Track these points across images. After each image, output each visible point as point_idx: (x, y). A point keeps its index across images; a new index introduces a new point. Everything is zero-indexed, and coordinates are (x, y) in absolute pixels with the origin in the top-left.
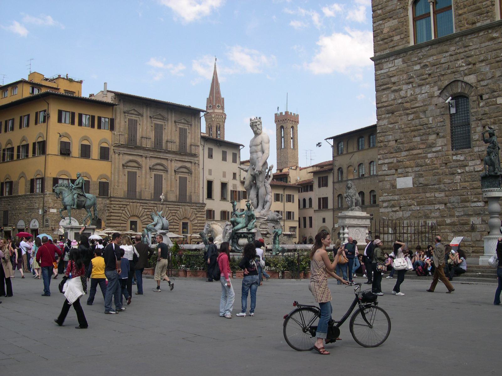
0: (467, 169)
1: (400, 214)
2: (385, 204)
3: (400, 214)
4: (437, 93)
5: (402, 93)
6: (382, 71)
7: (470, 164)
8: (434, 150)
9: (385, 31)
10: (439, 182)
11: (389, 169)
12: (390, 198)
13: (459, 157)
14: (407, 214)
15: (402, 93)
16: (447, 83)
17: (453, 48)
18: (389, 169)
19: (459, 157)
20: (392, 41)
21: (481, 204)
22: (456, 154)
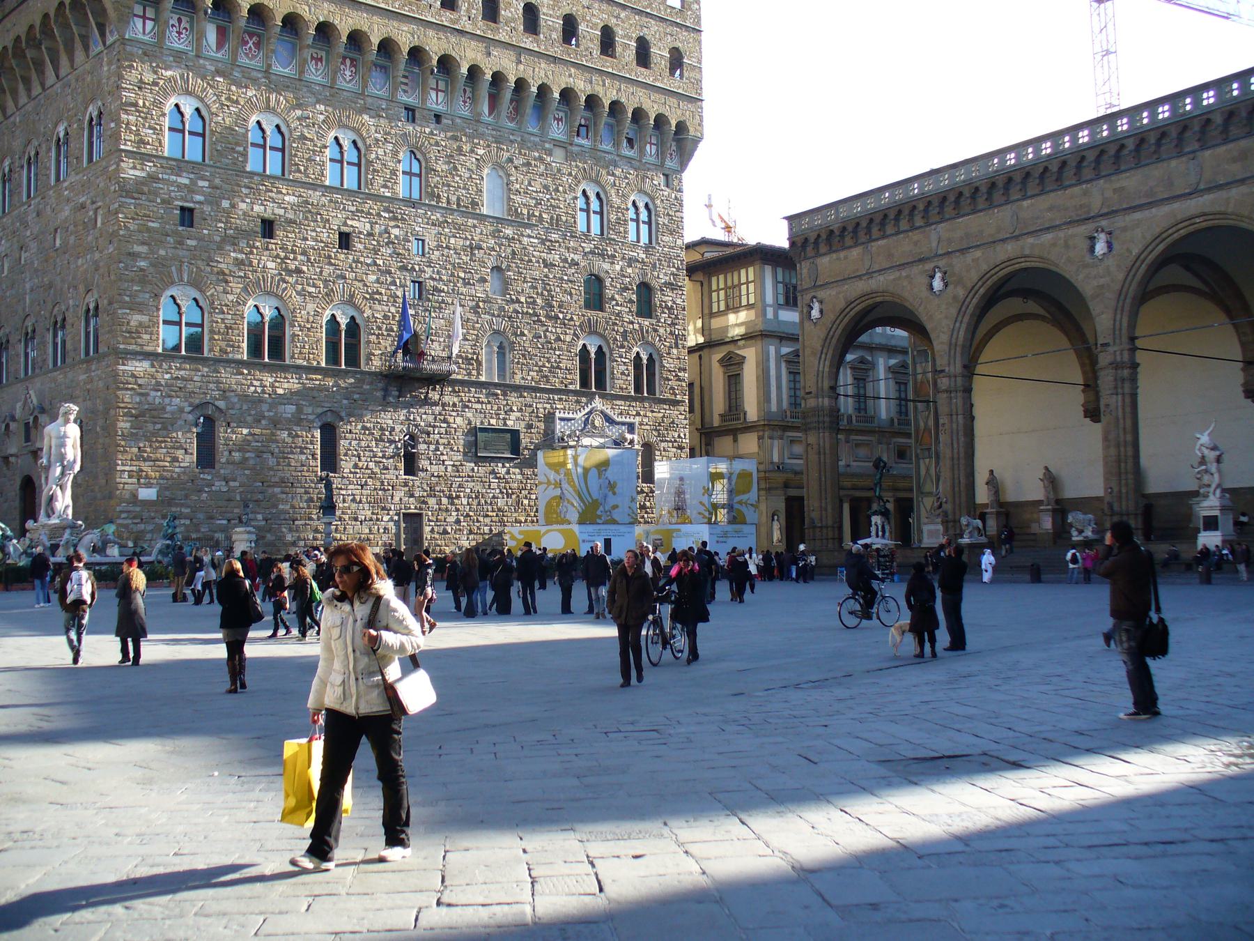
0: (214, 488)
1: (142, 527)
2: (123, 515)
3: (142, 527)
4: (189, 409)
5: (150, 399)
6: (126, 368)
7: (217, 483)
8: (182, 465)
9: (132, 323)
10: (186, 497)
11: (130, 477)
12: (132, 509)
13: (206, 476)
14: (150, 527)
15: (150, 399)
16: (197, 401)
17: (206, 369)
18: (130, 477)
19: (206, 476)
20: (140, 338)
21: (225, 522)
22: (203, 473)
